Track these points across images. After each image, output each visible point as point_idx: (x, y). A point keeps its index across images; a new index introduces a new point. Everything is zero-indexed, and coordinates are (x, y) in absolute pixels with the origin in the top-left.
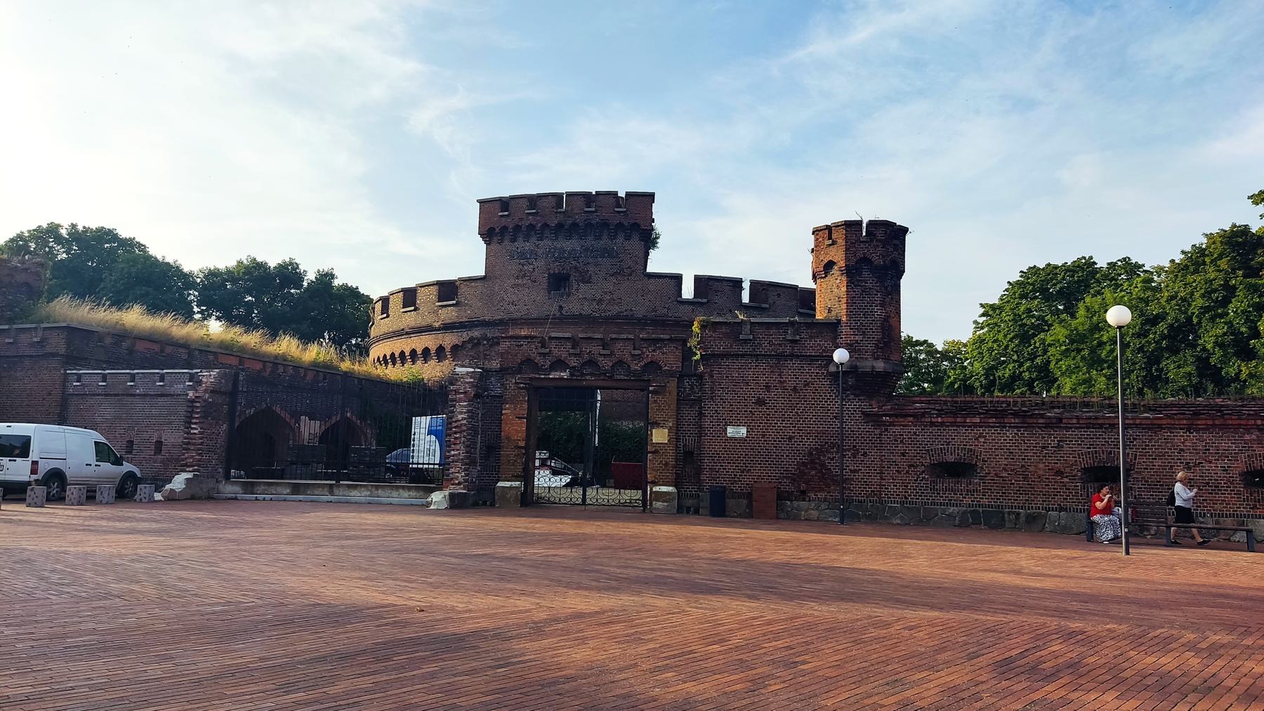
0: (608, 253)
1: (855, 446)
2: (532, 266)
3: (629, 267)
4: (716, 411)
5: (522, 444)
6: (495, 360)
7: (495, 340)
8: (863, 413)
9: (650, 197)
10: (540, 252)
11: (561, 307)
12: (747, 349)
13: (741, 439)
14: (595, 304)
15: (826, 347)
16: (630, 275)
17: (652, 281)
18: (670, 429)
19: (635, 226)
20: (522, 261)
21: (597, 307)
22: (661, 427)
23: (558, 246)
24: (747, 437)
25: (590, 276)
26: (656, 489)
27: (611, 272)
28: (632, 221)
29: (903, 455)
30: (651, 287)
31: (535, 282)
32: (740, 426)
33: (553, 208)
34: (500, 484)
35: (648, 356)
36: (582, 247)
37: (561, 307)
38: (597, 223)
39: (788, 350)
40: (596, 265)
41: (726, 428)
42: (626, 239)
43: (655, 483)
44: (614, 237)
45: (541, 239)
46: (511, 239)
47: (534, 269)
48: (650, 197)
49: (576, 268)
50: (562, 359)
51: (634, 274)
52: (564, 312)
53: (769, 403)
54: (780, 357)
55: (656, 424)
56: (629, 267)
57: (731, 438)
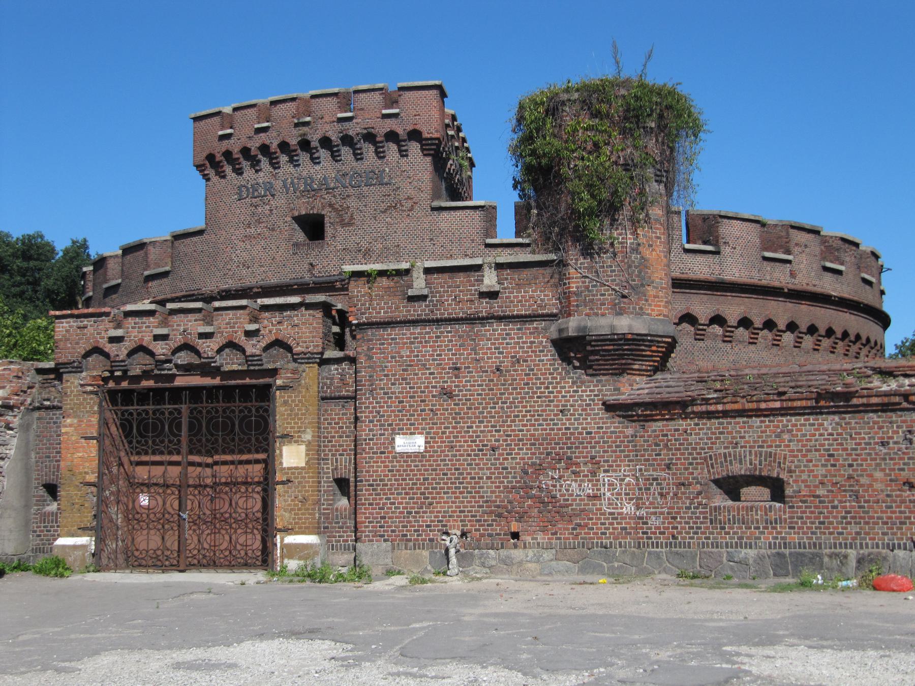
0: (377, 179)
1: (593, 458)
2: (268, 207)
4: (378, 412)
5: (92, 478)
8: (604, 404)
10: (278, 184)
12: (419, 310)
13: (417, 455)
15: (542, 300)
18: (309, 444)
22: (295, 442)
23: (305, 174)
24: (426, 451)
25: (352, 218)
26: (290, 539)
27: (383, 206)
28: (410, 128)
29: (668, 467)
30: (443, 226)
31: (273, 230)
32: (414, 434)
33: (293, 117)
34: (61, 541)
35: (270, 332)
36: (338, 171)
38: (358, 134)
39: (484, 307)
40: (360, 197)
41: (393, 439)
43: (287, 531)
47: (271, 211)
49: (331, 205)
50: (144, 344)
52: (315, 272)
53: (458, 395)
54: (471, 320)
55: (287, 437)
56: (409, 198)
57: (402, 454)
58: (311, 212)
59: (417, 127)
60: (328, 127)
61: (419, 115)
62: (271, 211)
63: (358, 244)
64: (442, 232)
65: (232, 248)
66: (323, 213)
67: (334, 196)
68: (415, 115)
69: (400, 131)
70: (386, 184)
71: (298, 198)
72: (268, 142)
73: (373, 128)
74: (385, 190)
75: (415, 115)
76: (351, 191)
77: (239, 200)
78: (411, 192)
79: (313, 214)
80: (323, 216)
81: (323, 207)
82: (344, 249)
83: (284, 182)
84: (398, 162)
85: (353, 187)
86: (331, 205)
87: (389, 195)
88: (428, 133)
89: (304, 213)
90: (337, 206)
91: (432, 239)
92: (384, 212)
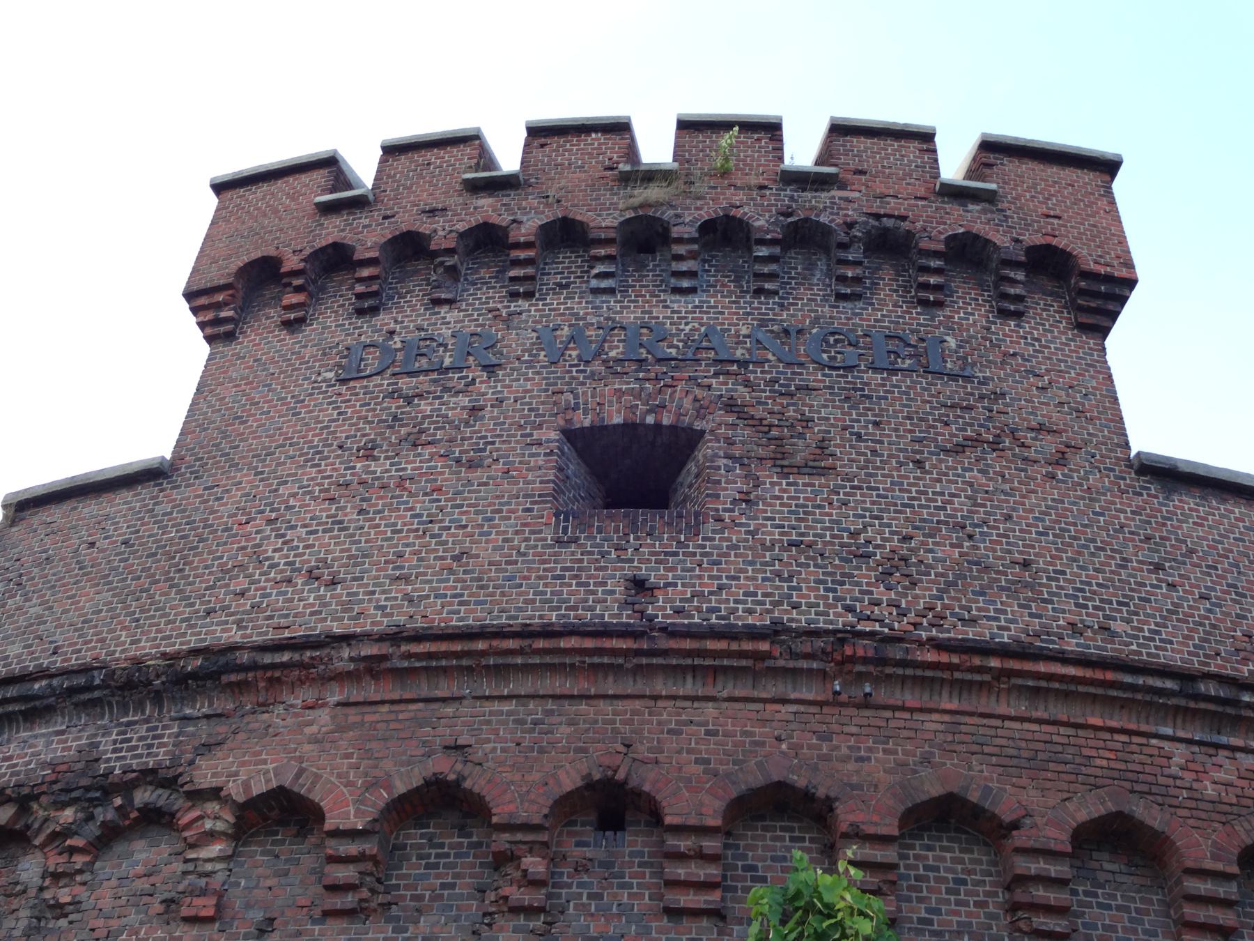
2: (464, 401)
3: (1040, 428)
7: (143, 796)
9: (1109, 167)
10: (516, 341)
11: (639, 585)
14: (865, 575)
16: (1060, 460)
17: (1186, 502)
20: (405, 384)
21: (880, 592)
23: (630, 316)
25: (822, 445)
27: (946, 435)
28: (1033, 238)
31: (472, 465)
36: (763, 323)
40: (855, 396)
42: (1004, 314)
46: (359, 296)
48: (1109, 167)
49: (731, 406)
51: (1076, 459)
58: (650, 420)
59: (1061, 243)
61: (1059, 218)
62: (475, 410)
63: (854, 535)
64: (1192, 552)
65: (270, 522)
66: (698, 425)
67: (747, 383)
69: (1001, 239)
70: (953, 377)
72: (503, 219)
73: (903, 218)
74: (951, 390)
75: (1048, 216)
76: (813, 376)
77: (343, 381)
78: (1046, 413)
79: (658, 426)
81: (701, 410)
82: (792, 544)
84: (988, 329)
85: (822, 366)
86: (731, 406)
87: (969, 408)
88: (1096, 262)
89: (617, 420)
90: (759, 412)
91: (1158, 567)
92: (959, 449)
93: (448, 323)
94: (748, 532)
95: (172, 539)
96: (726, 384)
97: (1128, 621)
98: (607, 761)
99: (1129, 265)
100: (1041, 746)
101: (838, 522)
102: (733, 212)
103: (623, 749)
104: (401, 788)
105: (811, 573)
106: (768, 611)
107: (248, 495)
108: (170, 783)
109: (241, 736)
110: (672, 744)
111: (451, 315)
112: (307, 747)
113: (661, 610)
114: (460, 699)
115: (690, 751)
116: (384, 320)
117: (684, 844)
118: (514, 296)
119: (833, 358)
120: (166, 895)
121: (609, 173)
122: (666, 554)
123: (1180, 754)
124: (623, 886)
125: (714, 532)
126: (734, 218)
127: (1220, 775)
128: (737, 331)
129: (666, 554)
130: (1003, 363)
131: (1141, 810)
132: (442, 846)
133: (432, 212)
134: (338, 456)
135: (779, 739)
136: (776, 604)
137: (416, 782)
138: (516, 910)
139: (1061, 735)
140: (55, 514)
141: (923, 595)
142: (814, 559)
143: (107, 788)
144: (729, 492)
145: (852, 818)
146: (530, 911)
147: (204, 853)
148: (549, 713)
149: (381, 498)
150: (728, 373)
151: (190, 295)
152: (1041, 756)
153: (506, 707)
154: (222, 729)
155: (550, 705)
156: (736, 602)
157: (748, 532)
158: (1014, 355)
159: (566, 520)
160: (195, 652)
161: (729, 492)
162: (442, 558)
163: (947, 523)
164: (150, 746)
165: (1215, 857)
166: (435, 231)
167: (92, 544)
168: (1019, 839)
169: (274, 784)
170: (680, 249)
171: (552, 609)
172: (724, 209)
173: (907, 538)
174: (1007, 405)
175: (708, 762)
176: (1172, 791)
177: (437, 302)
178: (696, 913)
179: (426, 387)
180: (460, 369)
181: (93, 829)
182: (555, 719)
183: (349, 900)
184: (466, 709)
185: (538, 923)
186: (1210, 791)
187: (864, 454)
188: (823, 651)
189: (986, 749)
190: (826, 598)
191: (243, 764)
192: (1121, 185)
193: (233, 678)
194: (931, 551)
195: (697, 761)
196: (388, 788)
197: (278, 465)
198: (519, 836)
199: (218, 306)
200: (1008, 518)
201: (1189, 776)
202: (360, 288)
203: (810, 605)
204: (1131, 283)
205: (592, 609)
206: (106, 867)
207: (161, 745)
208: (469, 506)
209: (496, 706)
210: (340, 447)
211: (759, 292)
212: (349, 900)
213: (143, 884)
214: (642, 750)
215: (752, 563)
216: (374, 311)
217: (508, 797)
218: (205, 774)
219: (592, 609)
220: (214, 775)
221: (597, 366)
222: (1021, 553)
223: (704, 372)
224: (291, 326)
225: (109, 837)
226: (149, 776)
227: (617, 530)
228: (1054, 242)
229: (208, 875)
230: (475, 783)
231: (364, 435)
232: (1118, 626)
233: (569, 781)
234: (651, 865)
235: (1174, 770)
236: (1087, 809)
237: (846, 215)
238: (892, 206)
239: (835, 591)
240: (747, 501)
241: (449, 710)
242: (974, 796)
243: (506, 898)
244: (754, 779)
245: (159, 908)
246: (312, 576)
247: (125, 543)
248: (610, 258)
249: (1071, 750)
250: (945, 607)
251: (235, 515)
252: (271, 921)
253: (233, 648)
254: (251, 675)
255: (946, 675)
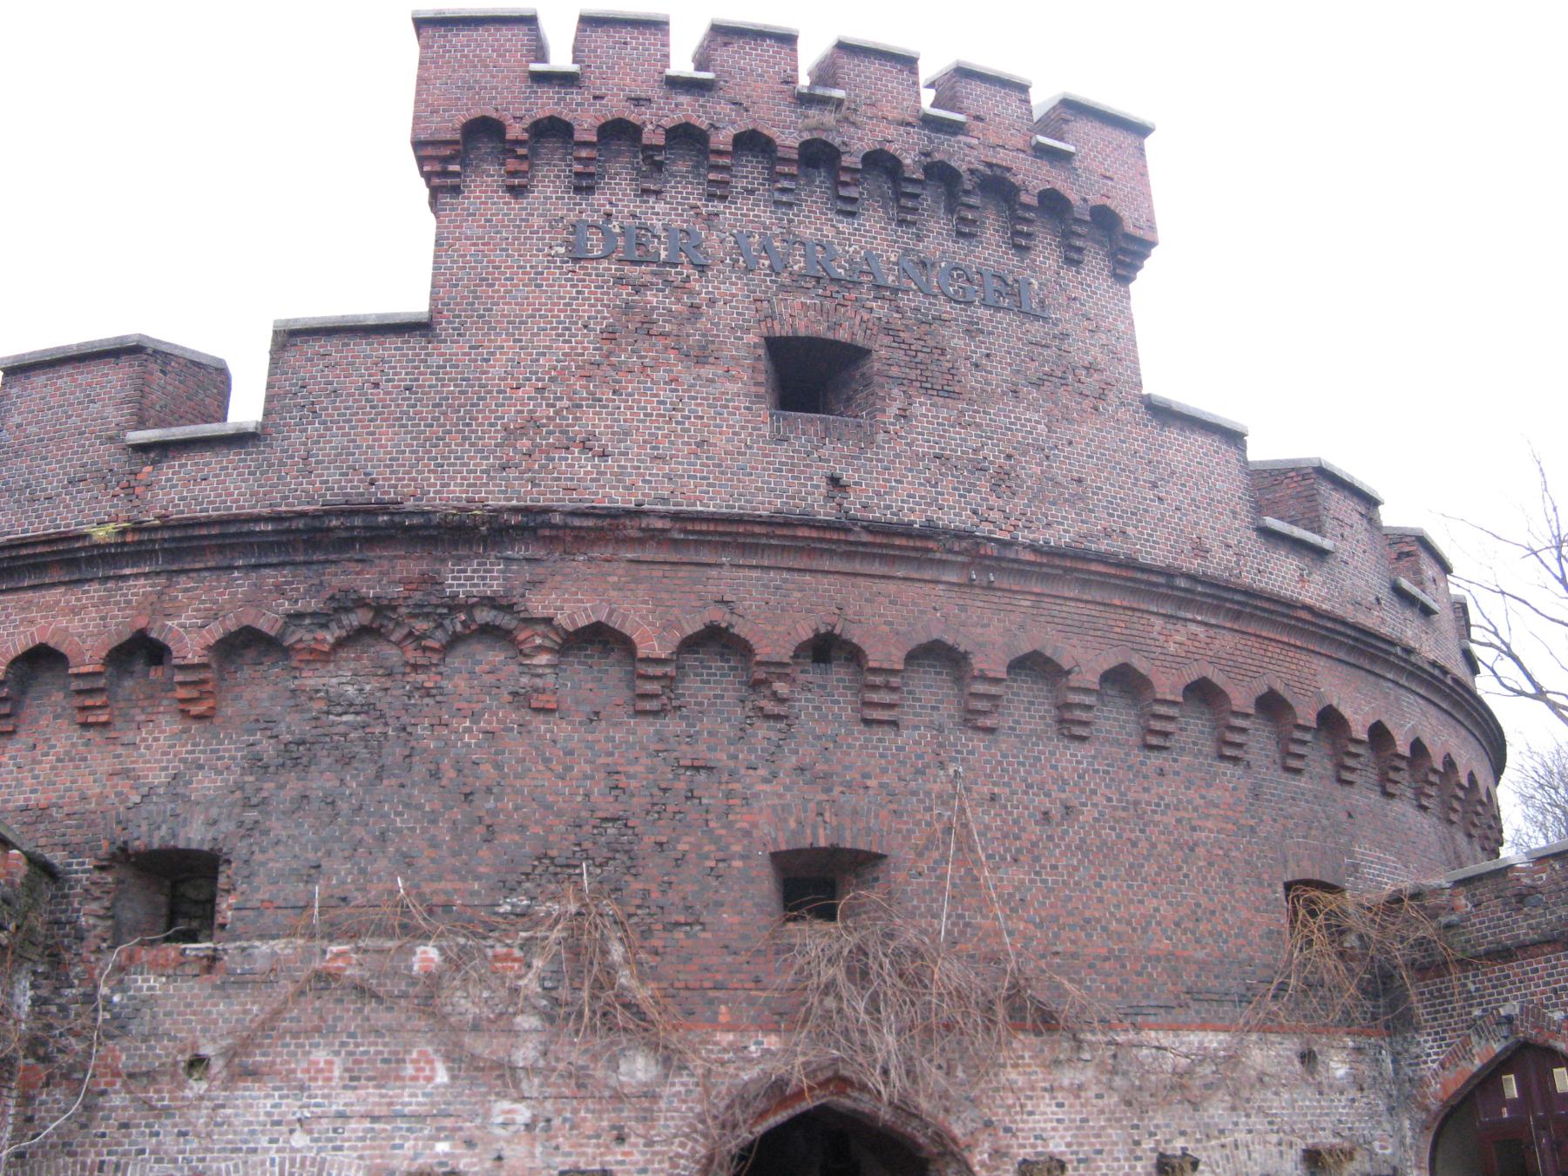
6: (475, 716)
7: (484, 616)
10: (715, 243)
11: (834, 481)
17: (1172, 435)
19: (1105, 220)
20: (633, 271)
21: (993, 500)
31: (701, 360)
37: (834, 481)
40: (972, 331)
42: (1070, 262)
44: (1021, 246)
45: (719, 192)
46: (578, 174)
60: (891, 132)
61: (1112, 179)
63: (975, 451)
64: (1173, 473)
68: (1105, 177)
69: (1074, 197)
70: (1037, 317)
71: (783, 288)
72: (702, 123)
73: (1009, 169)
75: (1105, 177)
80: (864, 353)
83: (740, 246)
85: (950, 299)
93: (660, 214)
94: (907, 444)
95: (452, 392)
96: (883, 308)
97: (1136, 527)
98: (828, 619)
99: (1152, 227)
100: (1085, 618)
101: (965, 440)
102: (887, 147)
103: (837, 611)
104: (689, 631)
105: (947, 483)
106: (925, 511)
107: (512, 360)
108: (509, 608)
109: (558, 578)
110: (868, 609)
111: (660, 207)
112: (613, 594)
113: (853, 505)
114: (721, 565)
115: (880, 615)
116: (598, 198)
117: (878, 680)
118: (711, 197)
119: (956, 292)
120: (511, 689)
121: (785, 87)
122: (853, 457)
123: (1158, 623)
124: (834, 702)
125: (884, 441)
126: (887, 153)
127: (1178, 638)
128: (888, 258)
129: (853, 457)
130: (1068, 306)
131: (1140, 664)
132: (710, 668)
133: (637, 101)
134: (585, 336)
135: (935, 609)
136: (930, 505)
137: (699, 627)
138: (768, 717)
139: (1094, 610)
140: (330, 346)
141: (1020, 502)
142: (951, 469)
143: (454, 606)
144: (893, 410)
145: (984, 666)
146: (778, 717)
147: (535, 661)
148: (785, 581)
149: (631, 382)
150: (883, 298)
151: (417, 145)
152: (1086, 625)
153: (755, 574)
154: (540, 570)
155: (785, 575)
156: (903, 501)
157: (907, 444)
158: (1075, 299)
159: (778, 421)
160: (515, 510)
161: (893, 410)
162: (688, 444)
163: (1033, 446)
164: (484, 578)
165: (1172, 693)
166: (644, 123)
167: (376, 385)
168: (1074, 681)
169: (594, 619)
170: (845, 178)
171: (777, 497)
172: (880, 142)
173: (1009, 457)
174: (1070, 346)
175: (891, 623)
176: (1154, 649)
177: (646, 191)
178: (880, 722)
179: (648, 278)
180: (675, 265)
181: (440, 637)
182: (790, 586)
183: (653, 705)
184: (725, 573)
185: (782, 725)
186: (1172, 648)
187: (980, 382)
188: (966, 550)
189: (1056, 620)
190: (960, 502)
191: (565, 601)
192: (1149, 142)
193: (547, 533)
194: (1024, 468)
195: (885, 623)
196: (681, 629)
197: (533, 335)
198: (772, 669)
199: (446, 160)
200: (1070, 443)
201: (1162, 638)
202: (578, 167)
203: (950, 508)
204: (1152, 244)
205: (804, 499)
206: (456, 660)
207: (492, 578)
208: (702, 398)
209: (747, 573)
210: (586, 327)
211: (901, 222)
212: (653, 705)
213: (489, 679)
214: (849, 613)
215: (911, 470)
216: (590, 190)
217: (765, 642)
218: (538, 605)
219: (804, 499)
220: (543, 608)
221: (785, 278)
222: (1077, 472)
223: (865, 293)
224: (517, 191)
225: (455, 640)
226: (491, 602)
227: (816, 434)
228: (1108, 202)
229: (539, 676)
230: (741, 629)
231: (605, 318)
232: (1130, 530)
233: (806, 634)
234: (850, 688)
235: (1155, 635)
236: (1110, 660)
237: (970, 162)
238: (1001, 157)
239: (965, 497)
240: (905, 417)
241: (714, 573)
242: (1048, 653)
243: (761, 709)
244: (922, 638)
245: (510, 698)
246: (585, 447)
247: (408, 388)
248: (791, 177)
249: (1102, 621)
250: (1033, 513)
251: (505, 379)
252: (597, 713)
253: (546, 510)
254: (561, 533)
255: (1037, 569)
